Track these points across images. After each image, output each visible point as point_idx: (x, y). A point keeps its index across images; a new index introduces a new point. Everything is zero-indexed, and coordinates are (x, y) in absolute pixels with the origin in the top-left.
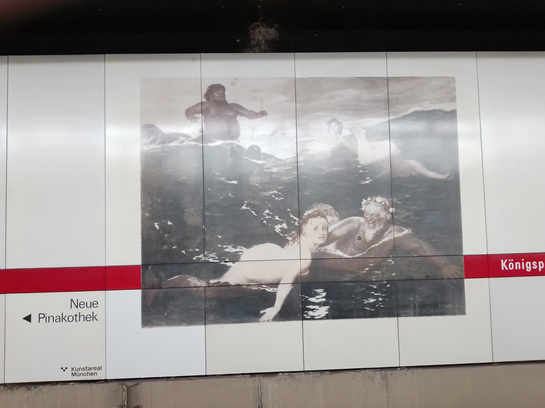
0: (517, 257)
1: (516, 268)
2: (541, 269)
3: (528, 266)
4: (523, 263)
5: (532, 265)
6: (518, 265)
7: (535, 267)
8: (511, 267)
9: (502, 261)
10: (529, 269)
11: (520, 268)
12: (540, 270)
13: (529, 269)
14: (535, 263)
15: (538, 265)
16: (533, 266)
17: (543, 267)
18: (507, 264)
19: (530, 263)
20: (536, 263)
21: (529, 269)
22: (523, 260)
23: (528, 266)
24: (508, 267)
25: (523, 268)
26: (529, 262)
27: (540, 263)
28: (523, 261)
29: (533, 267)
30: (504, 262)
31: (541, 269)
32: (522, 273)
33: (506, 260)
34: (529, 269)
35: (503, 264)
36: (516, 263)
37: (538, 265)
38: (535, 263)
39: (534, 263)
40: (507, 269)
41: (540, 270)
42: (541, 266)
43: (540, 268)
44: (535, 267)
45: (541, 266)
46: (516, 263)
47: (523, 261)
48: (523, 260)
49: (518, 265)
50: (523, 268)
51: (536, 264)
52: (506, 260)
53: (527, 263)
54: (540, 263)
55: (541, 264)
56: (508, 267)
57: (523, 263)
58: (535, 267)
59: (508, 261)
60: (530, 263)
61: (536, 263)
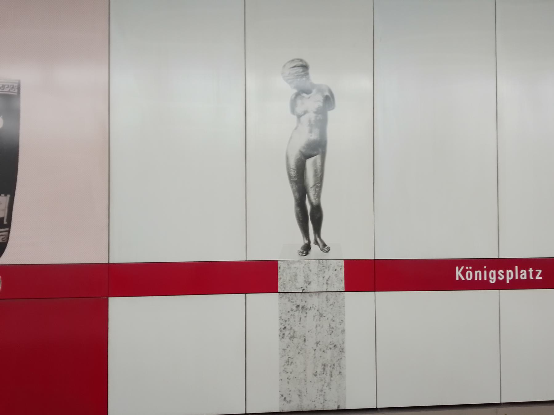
2: (510, 281)
4: (485, 272)
5: (497, 275)
6: (478, 274)
7: (501, 278)
9: (457, 268)
11: (480, 279)
12: (508, 282)
13: (493, 280)
14: (501, 273)
15: (505, 274)
17: (511, 278)
18: (463, 273)
19: (494, 272)
20: (503, 272)
21: (493, 280)
24: (465, 277)
26: (493, 270)
27: (508, 272)
29: (499, 278)
30: (459, 269)
32: (484, 285)
33: (463, 267)
34: (493, 280)
35: (458, 273)
36: (476, 272)
37: (505, 274)
38: (501, 273)
39: (501, 272)
41: (508, 282)
42: (510, 276)
43: (508, 279)
44: (501, 277)
45: (510, 276)
46: (476, 272)
47: (485, 269)
49: (478, 274)
51: (502, 274)
52: (463, 267)
53: (491, 271)
54: (508, 272)
55: (510, 274)
57: (485, 272)
59: (465, 268)
60: (494, 272)
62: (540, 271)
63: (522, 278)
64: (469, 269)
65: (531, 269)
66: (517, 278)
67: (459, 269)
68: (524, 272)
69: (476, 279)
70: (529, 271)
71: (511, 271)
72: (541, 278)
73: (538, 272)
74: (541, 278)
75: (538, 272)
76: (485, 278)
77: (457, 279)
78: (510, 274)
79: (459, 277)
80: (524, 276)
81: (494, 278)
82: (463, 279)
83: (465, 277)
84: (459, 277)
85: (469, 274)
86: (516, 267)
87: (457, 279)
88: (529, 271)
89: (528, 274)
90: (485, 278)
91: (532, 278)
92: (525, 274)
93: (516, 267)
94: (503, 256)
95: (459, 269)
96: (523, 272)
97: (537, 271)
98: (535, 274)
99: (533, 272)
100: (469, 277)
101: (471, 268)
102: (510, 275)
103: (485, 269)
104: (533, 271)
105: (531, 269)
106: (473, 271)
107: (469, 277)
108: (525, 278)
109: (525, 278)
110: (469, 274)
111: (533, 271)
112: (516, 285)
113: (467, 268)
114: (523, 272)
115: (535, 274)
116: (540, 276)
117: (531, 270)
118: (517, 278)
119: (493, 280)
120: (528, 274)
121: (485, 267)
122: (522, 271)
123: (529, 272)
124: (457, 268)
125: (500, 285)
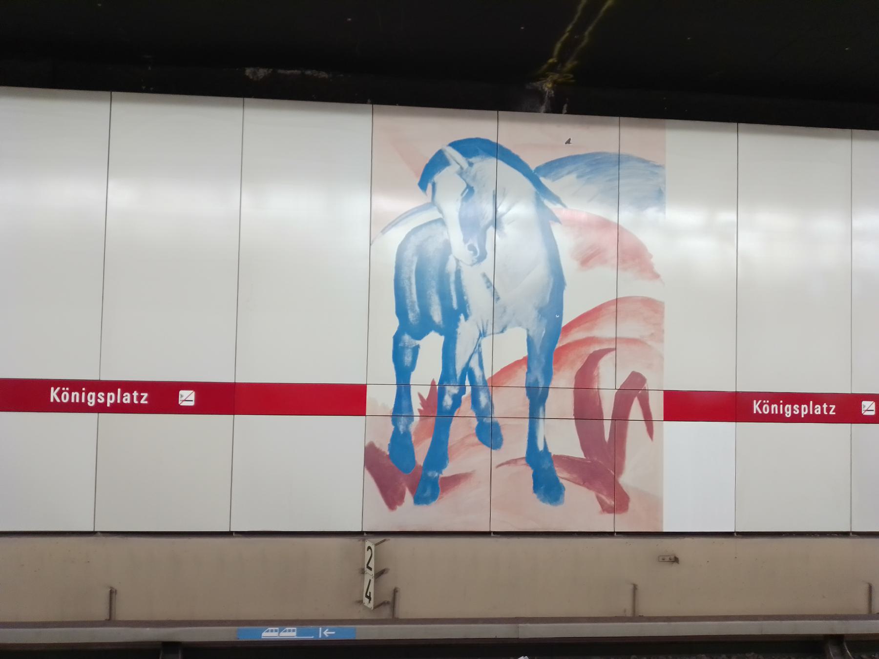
0: (75, 385)
1: (73, 401)
2: (111, 404)
4: (83, 394)
5: (97, 398)
6: (75, 396)
8: (65, 398)
9: (755, 402)
10: (91, 403)
11: (77, 401)
12: (108, 405)
13: (91, 403)
16: (99, 398)
17: (113, 401)
18: (761, 406)
20: (103, 394)
21: (91, 403)
22: (84, 389)
25: (83, 401)
26: (93, 392)
28: (83, 391)
29: (99, 400)
32: (81, 408)
33: (760, 401)
34: (91, 403)
35: (756, 407)
36: (73, 394)
37: (105, 397)
38: (101, 395)
41: (108, 405)
43: (109, 402)
44: (101, 400)
47: (83, 391)
49: (75, 396)
50: (83, 401)
52: (760, 401)
53: (90, 394)
57: (83, 394)
58: (101, 400)
59: (61, 389)
60: (94, 394)
62: (833, 407)
63: (124, 401)
64: (66, 391)
65: (825, 404)
66: (119, 401)
67: (55, 390)
68: (127, 395)
69: (773, 412)
70: (823, 406)
71: (113, 394)
74: (146, 402)
76: (781, 412)
77: (52, 400)
79: (54, 399)
80: (818, 411)
82: (58, 400)
83: (60, 398)
84: (54, 399)
86: (119, 390)
87: (755, 412)
89: (132, 397)
90: (781, 412)
91: (136, 402)
92: (129, 397)
93: (119, 390)
94: (104, 378)
95: (55, 390)
96: (818, 408)
97: (831, 406)
98: (829, 409)
99: (137, 396)
100: (766, 410)
101: (67, 389)
102: (111, 399)
103: (782, 404)
104: (827, 406)
105: (135, 392)
107: (65, 398)
108: (819, 413)
109: (129, 401)
111: (137, 394)
112: (119, 408)
113: (64, 389)
114: (818, 408)
115: (829, 409)
116: (146, 400)
117: (135, 394)
118: (119, 401)
120: (132, 397)
121: (781, 402)
122: (816, 406)
124: (52, 389)
125: (100, 408)
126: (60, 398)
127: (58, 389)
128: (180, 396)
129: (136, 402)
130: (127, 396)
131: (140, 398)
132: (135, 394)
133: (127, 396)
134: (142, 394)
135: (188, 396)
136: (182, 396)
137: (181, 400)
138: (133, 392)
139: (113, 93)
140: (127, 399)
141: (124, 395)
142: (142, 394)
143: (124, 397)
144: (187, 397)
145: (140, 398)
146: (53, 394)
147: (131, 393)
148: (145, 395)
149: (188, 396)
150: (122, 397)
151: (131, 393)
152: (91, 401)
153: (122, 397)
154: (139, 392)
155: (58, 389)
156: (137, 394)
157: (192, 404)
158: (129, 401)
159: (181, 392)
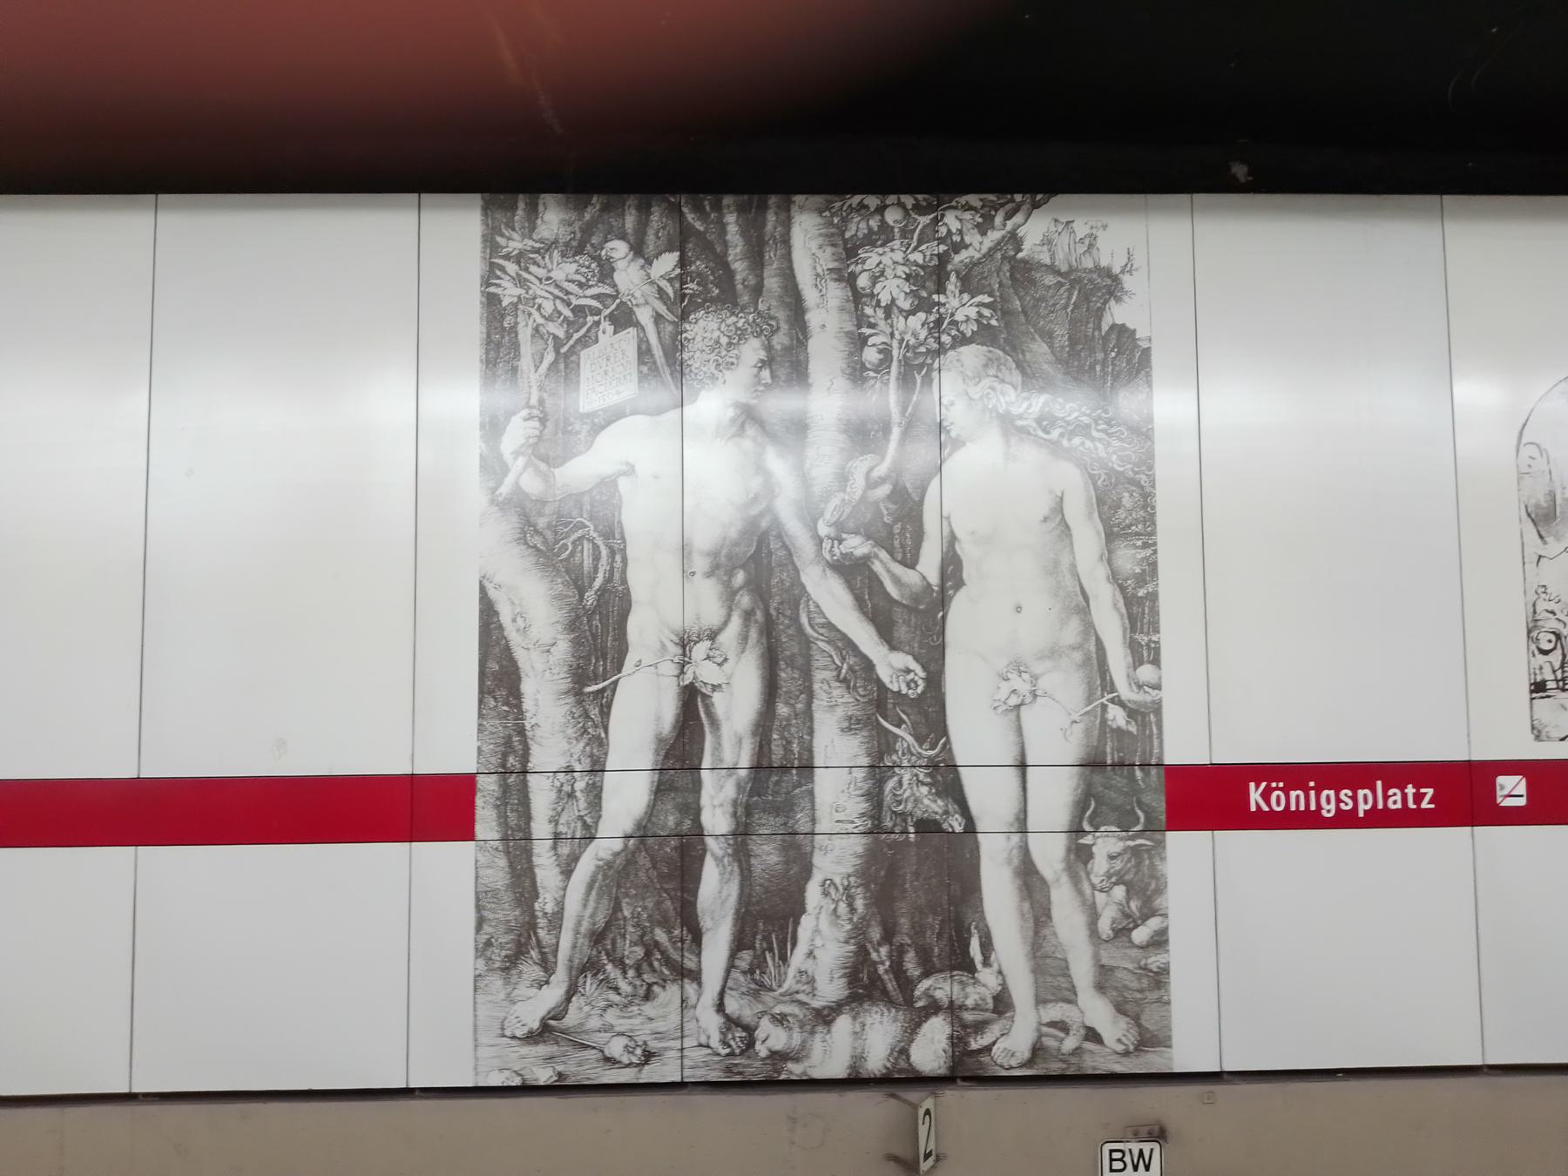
1: (1293, 808)
2: (1365, 811)
3: (1328, 801)
4: (1312, 793)
5: (1339, 801)
6: (1298, 797)
8: (1278, 803)
11: (1302, 808)
12: (1361, 814)
13: (1329, 810)
15: (1354, 798)
16: (1343, 802)
17: (1368, 807)
20: (1350, 793)
23: (1328, 801)
25: (1313, 807)
26: (1330, 789)
27: (1361, 793)
28: (1312, 788)
29: (1342, 806)
31: (1365, 811)
32: (1310, 820)
34: (1329, 810)
36: (1293, 794)
37: (1354, 798)
38: (1346, 795)
39: (1345, 793)
40: (1266, 809)
41: (1361, 814)
42: (1366, 802)
43: (1363, 808)
44: (1346, 804)
45: (1366, 802)
46: (1293, 794)
47: (1312, 788)
48: (1312, 784)
49: (1298, 797)
50: (1313, 807)
53: (1325, 792)
54: (1361, 793)
55: (1365, 797)
56: (1268, 802)
57: (1312, 793)
58: (1346, 804)
60: (1332, 793)
61: (1350, 794)
63: (1391, 806)
64: (1277, 788)
66: (1380, 806)
67: (1257, 787)
71: (1367, 791)
72: (1432, 806)
73: (1425, 794)
74: (1432, 806)
75: (1425, 794)
77: (1253, 808)
78: (1365, 797)
79: (1257, 805)
81: (1332, 806)
82: (1266, 809)
83: (1268, 802)
84: (1257, 805)
85: (1278, 798)
86: (1379, 784)
88: (1406, 791)
89: (1404, 797)
91: (1412, 805)
92: (1398, 798)
93: (1379, 784)
95: (1257, 787)
99: (1414, 794)
101: (1281, 785)
105: (1410, 786)
106: (1286, 791)
107: (1278, 803)
109: (1399, 806)
110: (1278, 797)
111: (1414, 790)
112: (1379, 819)
113: (1274, 785)
116: (1429, 803)
117: (1410, 790)
118: (1380, 806)
119: (1329, 811)
120: (1404, 797)
123: (1406, 793)
124: (1252, 785)
125: (1345, 820)
126: (1268, 802)
127: (1264, 784)
128: (1498, 788)
129: (1412, 805)
130: (1395, 794)
131: (1419, 798)
132: (1410, 790)
133: (1395, 794)
134: (1423, 790)
135: (1514, 787)
136: (1502, 788)
137: (1501, 796)
138: (1406, 788)
139: (1445, 197)
140: (1395, 802)
141: (1391, 792)
142: (1423, 790)
143: (1391, 796)
144: (1511, 791)
145: (1419, 798)
146: (1255, 795)
147: (1402, 789)
148: (1430, 792)
149: (1514, 787)
150: (1386, 798)
151: (1402, 789)
152: (1328, 807)
153: (1386, 798)
154: (1417, 787)
155: (1264, 784)
156: (1414, 790)
157: (1522, 802)
158: (1399, 806)
159: (1501, 780)
